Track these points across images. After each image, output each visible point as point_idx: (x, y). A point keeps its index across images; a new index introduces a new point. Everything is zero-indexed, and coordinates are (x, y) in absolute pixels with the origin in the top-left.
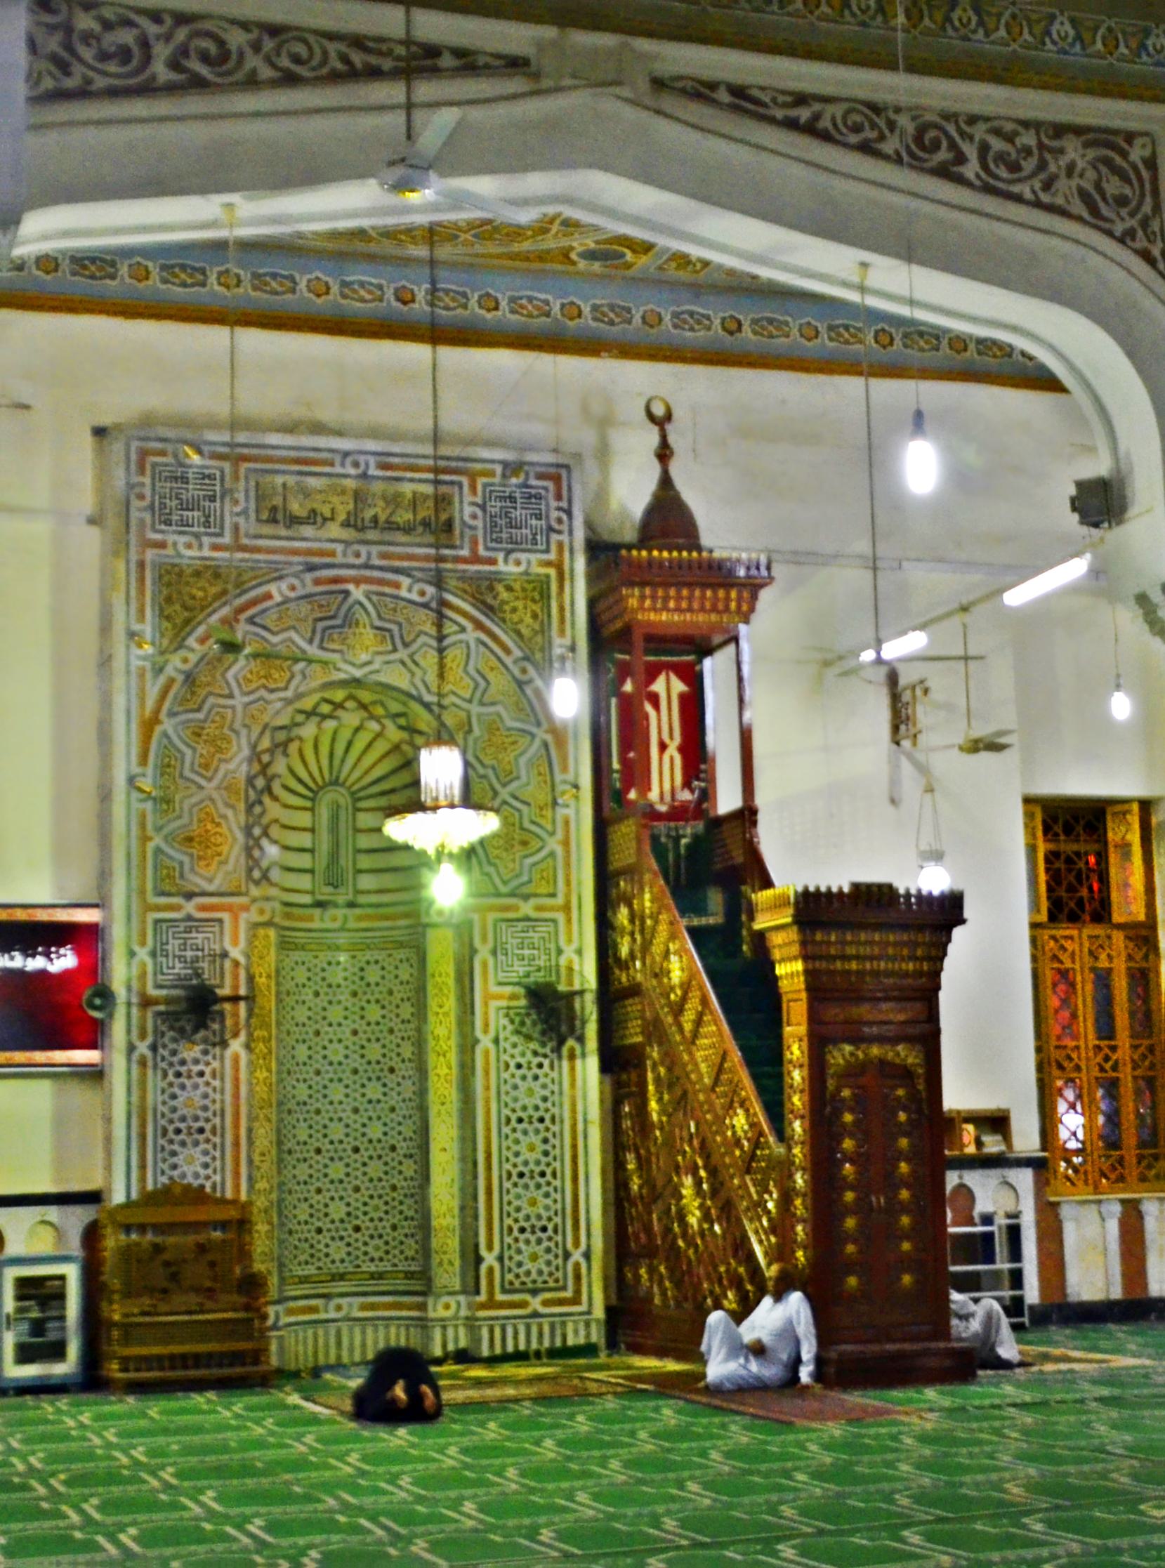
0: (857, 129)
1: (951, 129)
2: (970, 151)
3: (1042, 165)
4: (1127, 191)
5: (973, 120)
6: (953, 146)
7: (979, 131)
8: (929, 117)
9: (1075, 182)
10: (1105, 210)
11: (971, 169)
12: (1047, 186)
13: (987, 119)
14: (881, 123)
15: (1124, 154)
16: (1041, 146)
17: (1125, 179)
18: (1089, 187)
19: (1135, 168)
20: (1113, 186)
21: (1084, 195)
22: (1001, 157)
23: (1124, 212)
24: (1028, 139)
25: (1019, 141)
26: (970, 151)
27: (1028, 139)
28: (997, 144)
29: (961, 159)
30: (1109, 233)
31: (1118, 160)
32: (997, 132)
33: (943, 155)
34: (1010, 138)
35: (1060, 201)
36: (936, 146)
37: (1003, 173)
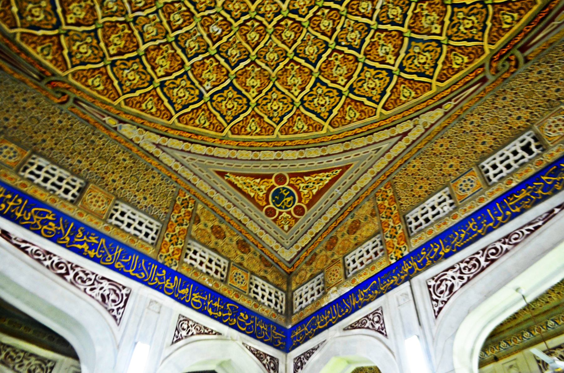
0: (39, 255)
1: (69, 266)
3: (93, 284)
4: (117, 299)
6: (67, 269)
8: (63, 261)
9: (101, 292)
10: (107, 301)
11: (70, 277)
14: (48, 257)
15: (120, 291)
16: (95, 279)
17: (117, 295)
18: (106, 295)
19: (122, 295)
20: (113, 297)
21: (103, 296)
22: (80, 278)
23: (113, 304)
25: (89, 276)
27: (93, 277)
28: (81, 274)
29: (68, 273)
30: (106, 308)
32: (84, 272)
33: (63, 271)
34: (87, 274)
35: (94, 295)
36: (62, 268)
37: (79, 281)
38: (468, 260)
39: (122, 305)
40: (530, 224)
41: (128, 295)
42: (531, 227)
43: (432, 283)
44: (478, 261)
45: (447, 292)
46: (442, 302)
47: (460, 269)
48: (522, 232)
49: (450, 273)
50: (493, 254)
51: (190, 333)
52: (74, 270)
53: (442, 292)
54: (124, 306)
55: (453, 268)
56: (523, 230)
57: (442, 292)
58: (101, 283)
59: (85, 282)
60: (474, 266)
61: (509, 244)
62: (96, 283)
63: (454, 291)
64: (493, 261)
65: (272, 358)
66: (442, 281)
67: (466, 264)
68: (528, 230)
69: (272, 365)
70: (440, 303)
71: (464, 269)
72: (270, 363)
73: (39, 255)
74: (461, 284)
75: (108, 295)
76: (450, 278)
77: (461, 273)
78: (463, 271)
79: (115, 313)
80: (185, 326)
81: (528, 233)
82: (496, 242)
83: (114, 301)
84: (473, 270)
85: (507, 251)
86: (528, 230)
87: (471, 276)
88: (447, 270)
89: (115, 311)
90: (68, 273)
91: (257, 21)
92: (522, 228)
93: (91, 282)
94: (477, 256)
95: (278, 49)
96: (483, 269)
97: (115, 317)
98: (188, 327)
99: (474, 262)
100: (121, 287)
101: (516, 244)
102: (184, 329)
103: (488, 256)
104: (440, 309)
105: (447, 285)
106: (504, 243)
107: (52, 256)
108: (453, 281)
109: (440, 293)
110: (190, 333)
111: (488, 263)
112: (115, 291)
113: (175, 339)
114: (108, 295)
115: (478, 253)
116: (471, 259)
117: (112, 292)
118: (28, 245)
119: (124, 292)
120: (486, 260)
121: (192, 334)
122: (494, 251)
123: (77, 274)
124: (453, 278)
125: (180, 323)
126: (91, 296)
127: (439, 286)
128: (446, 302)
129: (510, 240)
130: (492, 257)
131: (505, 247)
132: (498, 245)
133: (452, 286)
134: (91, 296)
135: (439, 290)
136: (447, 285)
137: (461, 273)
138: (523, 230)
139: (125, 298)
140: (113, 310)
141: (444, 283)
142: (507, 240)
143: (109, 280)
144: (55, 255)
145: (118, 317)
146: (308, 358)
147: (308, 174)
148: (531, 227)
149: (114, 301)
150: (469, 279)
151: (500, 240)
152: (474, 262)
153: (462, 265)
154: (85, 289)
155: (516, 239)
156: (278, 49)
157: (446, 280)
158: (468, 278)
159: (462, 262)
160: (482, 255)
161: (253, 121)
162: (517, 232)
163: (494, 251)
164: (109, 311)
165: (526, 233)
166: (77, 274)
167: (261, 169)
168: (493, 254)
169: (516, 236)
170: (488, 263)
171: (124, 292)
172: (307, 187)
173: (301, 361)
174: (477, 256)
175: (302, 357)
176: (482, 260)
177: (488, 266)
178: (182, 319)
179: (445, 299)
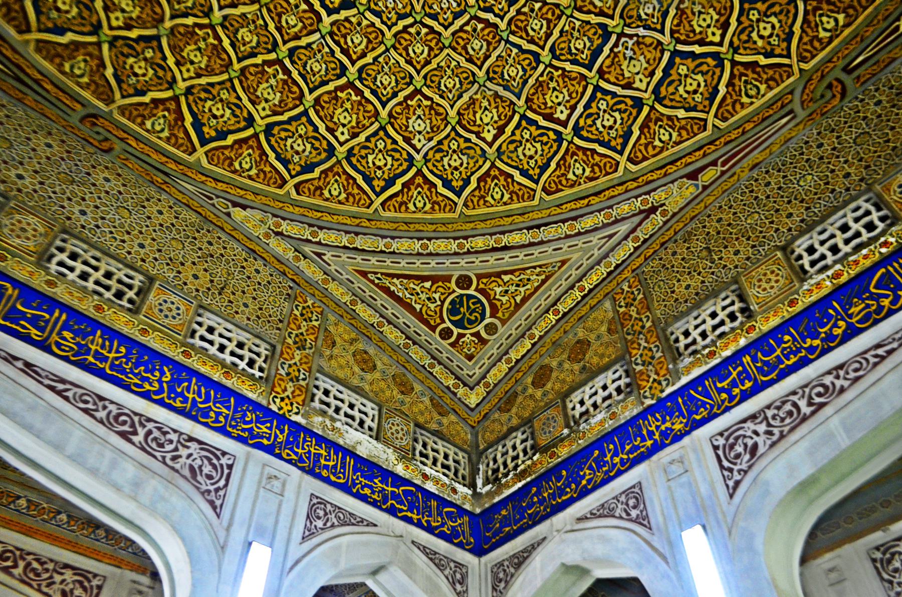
1: (136, 419)
2: (142, 432)
3: (176, 449)
4: (214, 474)
5: (149, 420)
6: (133, 425)
7: (150, 426)
9: (189, 461)
10: (199, 478)
11: (139, 438)
12: (174, 459)
13: (156, 422)
16: (179, 441)
18: (196, 467)
20: (207, 469)
21: (192, 468)
22: (155, 439)
23: (208, 482)
24: (174, 437)
25: (168, 436)
26: (142, 432)
29: (135, 433)
30: (198, 488)
31: (215, 461)
32: (159, 429)
33: (126, 428)
35: (177, 466)
36: (124, 423)
37: (154, 445)
38: (778, 404)
39: (222, 483)
40: (878, 346)
41: (230, 467)
42: (880, 352)
43: (721, 441)
44: (795, 405)
45: (747, 457)
46: (739, 471)
47: (766, 418)
48: (867, 360)
49: (749, 425)
50: (819, 395)
51: (329, 524)
52: (144, 426)
53: (738, 456)
54: (226, 485)
55: (753, 417)
56: (867, 356)
57: (738, 456)
58: (188, 447)
59: (161, 446)
60: (790, 414)
61: (845, 379)
62: (180, 447)
63: (758, 454)
64: (822, 406)
65: (459, 565)
66: (737, 439)
67: (776, 412)
68: (876, 356)
69: (458, 576)
70: (735, 473)
71: (774, 417)
72: (455, 572)
73: (86, 402)
74: (769, 442)
75: (200, 467)
76: (749, 433)
77: (769, 425)
78: (772, 422)
79: (212, 496)
80: (321, 513)
81: (876, 360)
82: (823, 375)
83: (209, 477)
84: (788, 421)
85: (842, 390)
86: (876, 356)
87: (786, 429)
88: (744, 421)
89: (213, 493)
90: (135, 433)
91: (425, 26)
92: (866, 352)
93: (171, 447)
94: (794, 398)
95: (460, 70)
96: (805, 419)
97: (212, 503)
98: (326, 514)
99: (788, 407)
100: (218, 453)
101: (857, 379)
102: (319, 518)
103: (810, 398)
104: (737, 483)
105: (746, 445)
106: (838, 377)
107: (107, 403)
108: (756, 438)
109: (736, 457)
110: (329, 524)
111: (812, 408)
112: (209, 460)
113: (307, 533)
114: (200, 467)
115: (794, 393)
116: (784, 403)
117: (206, 462)
118: (68, 386)
119: (224, 461)
120: (810, 404)
121: (333, 526)
122: (821, 389)
123: (150, 432)
124: (756, 433)
125: (312, 508)
126: (173, 468)
127: (732, 447)
128: (746, 472)
129: (847, 373)
130: (818, 400)
131: (838, 383)
132: (827, 380)
133: (755, 446)
134: (173, 468)
135: (732, 454)
136: (746, 445)
137: (769, 425)
138: (867, 356)
139: (226, 471)
140: (209, 492)
141: (740, 441)
142: (842, 373)
143: (200, 442)
144: (112, 402)
145: (218, 503)
146: (518, 566)
147: (506, 273)
148: (880, 352)
149: (209, 477)
150: (782, 436)
151: (829, 373)
152: (788, 407)
153: (770, 413)
154: (164, 458)
155: (856, 370)
156: (460, 70)
157: (745, 436)
158: (781, 432)
159: (768, 407)
160: (803, 396)
161: (496, 185)
162: (858, 359)
163: (821, 389)
164: (203, 493)
165: (873, 360)
166: (150, 432)
167: (432, 267)
168: (819, 395)
169: (857, 365)
170: (812, 408)
171: (224, 461)
172: (506, 292)
173: (505, 571)
174: (794, 398)
175: (506, 563)
176: (803, 404)
177: (813, 413)
178: (315, 501)
179: (744, 466)
